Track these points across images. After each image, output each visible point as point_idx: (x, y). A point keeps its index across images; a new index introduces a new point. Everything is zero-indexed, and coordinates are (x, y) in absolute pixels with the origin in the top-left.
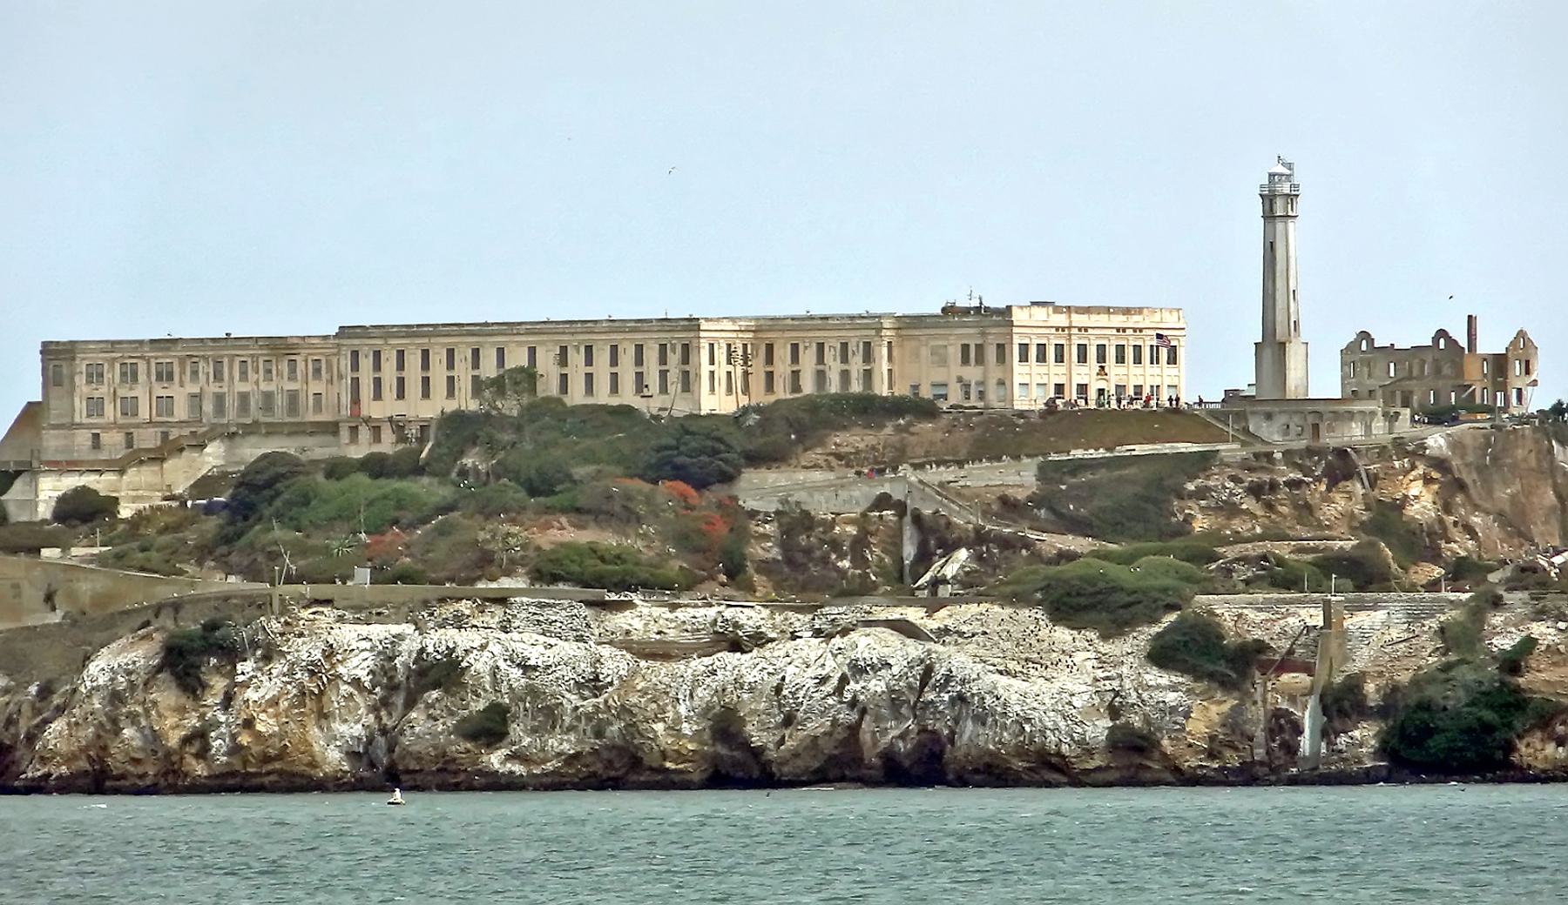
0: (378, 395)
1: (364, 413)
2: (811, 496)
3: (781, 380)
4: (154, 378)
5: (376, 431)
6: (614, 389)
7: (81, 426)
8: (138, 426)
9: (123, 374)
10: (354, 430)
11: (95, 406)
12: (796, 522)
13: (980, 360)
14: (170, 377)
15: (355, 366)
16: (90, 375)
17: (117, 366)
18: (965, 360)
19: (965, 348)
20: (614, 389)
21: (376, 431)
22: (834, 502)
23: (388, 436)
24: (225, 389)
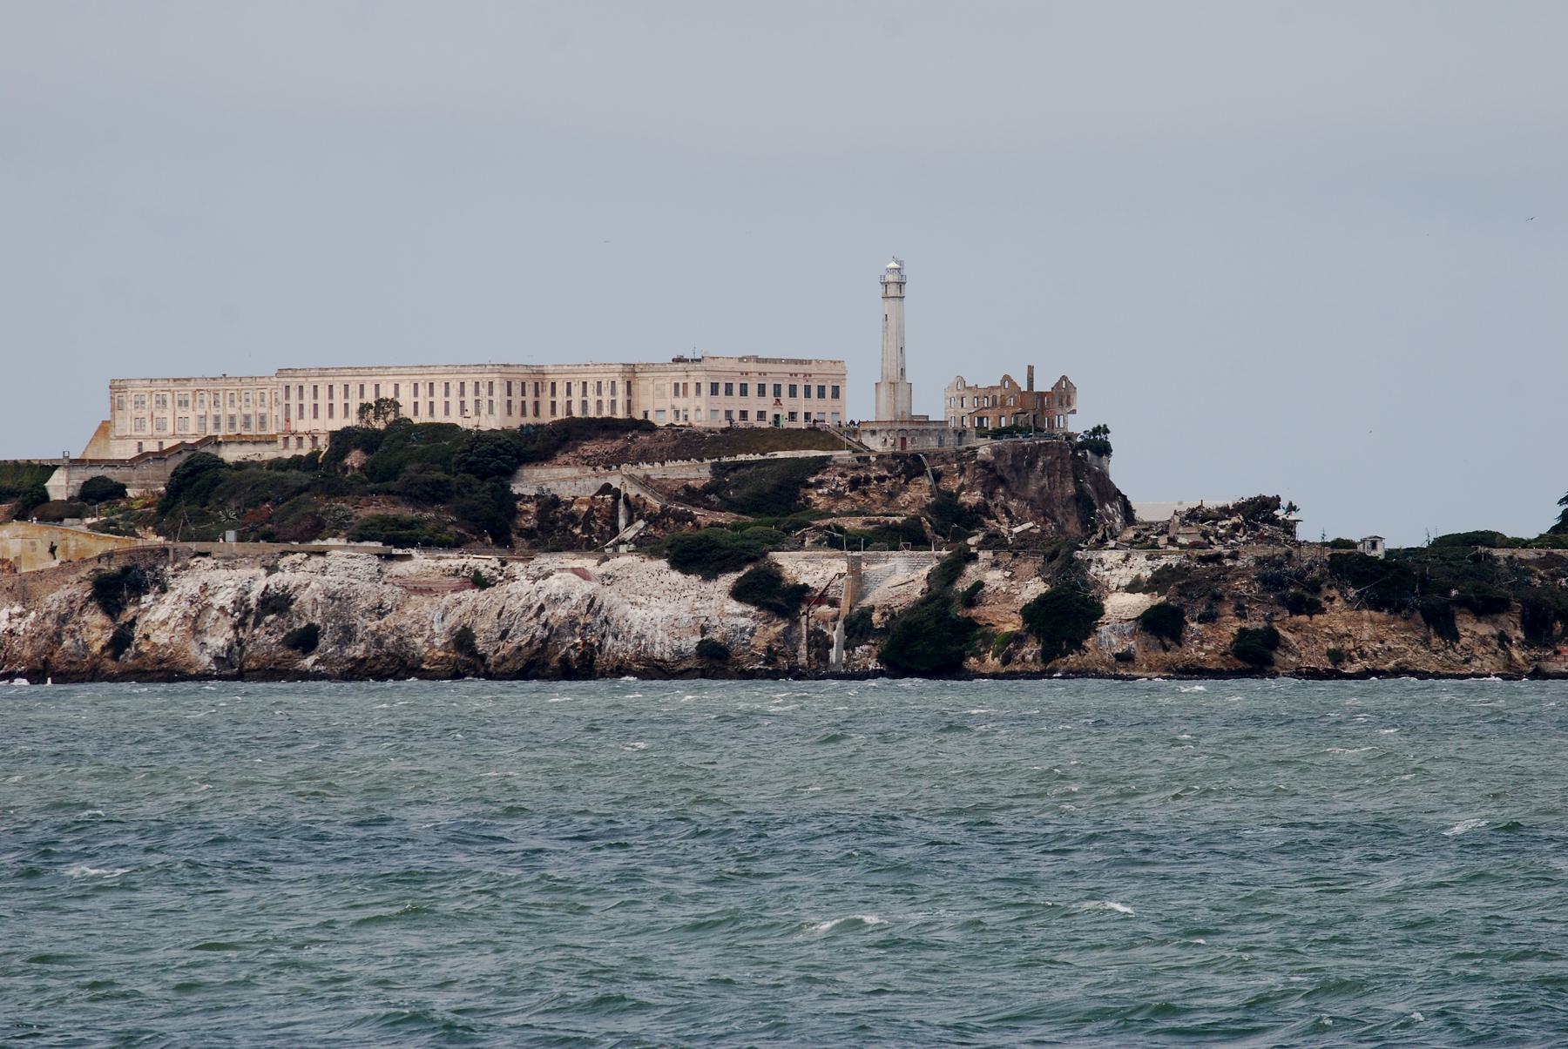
0: (301, 416)
4: (176, 405)
5: (300, 439)
6: (447, 412)
7: (130, 437)
9: (158, 402)
10: (286, 439)
11: (140, 422)
12: (549, 504)
13: (685, 394)
14: (186, 403)
15: (287, 397)
17: (154, 396)
18: (677, 394)
19: (677, 385)
20: (447, 412)
21: (300, 439)
23: (307, 443)
24: (221, 413)
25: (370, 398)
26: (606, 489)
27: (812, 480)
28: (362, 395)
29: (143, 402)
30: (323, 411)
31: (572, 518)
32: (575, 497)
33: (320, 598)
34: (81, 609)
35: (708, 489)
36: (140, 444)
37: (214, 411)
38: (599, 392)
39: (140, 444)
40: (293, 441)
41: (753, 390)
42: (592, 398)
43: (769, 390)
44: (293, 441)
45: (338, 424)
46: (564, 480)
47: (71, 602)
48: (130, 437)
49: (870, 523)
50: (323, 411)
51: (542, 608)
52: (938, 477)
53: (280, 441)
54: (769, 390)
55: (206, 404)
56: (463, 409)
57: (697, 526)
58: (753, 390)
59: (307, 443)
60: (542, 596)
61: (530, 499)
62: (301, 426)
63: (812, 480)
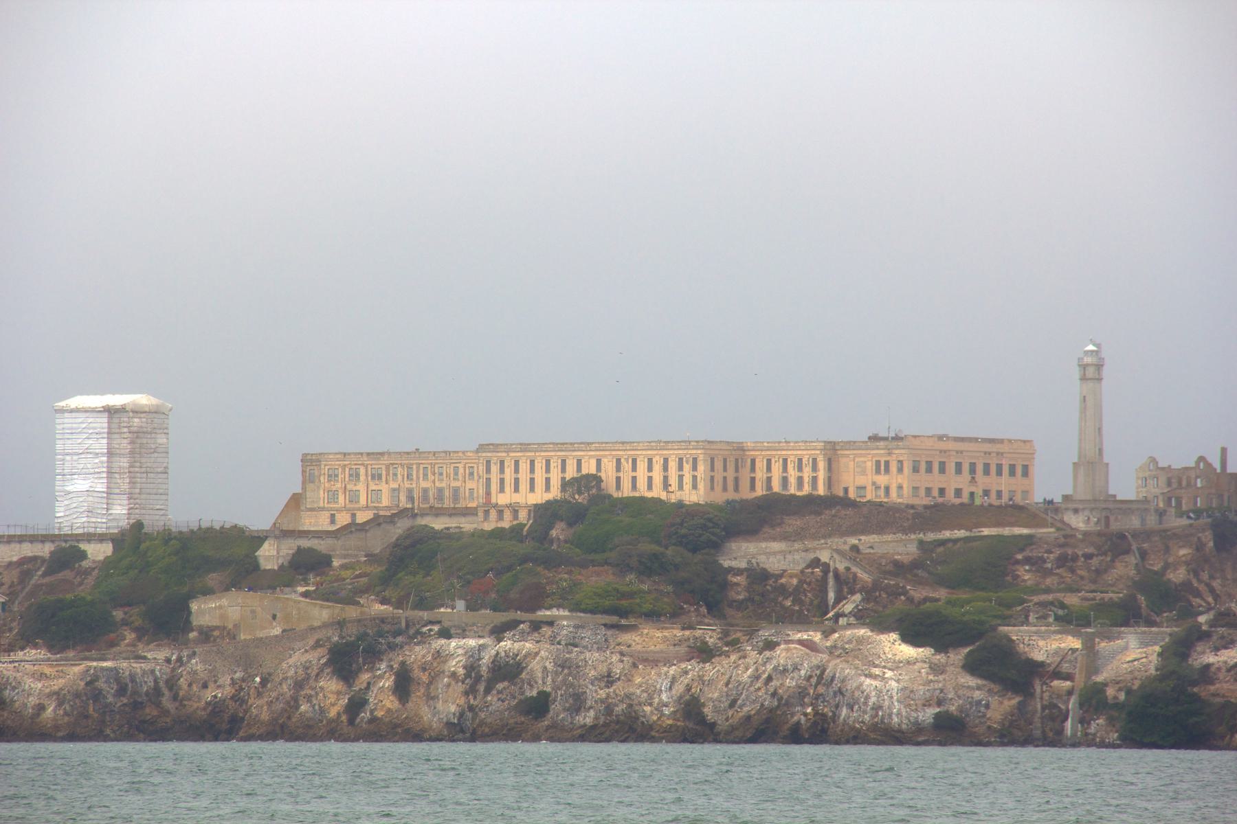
0: (502, 490)
1: (493, 501)
2: (768, 559)
3: (760, 483)
4: (370, 478)
5: (500, 513)
6: (650, 487)
7: (323, 509)
8: (359, 509)
9: (350, 475)
10: (487, 513)
11: (333, 495)
12: (759, 576)
13: (887, 470)
14: (380, 477)
15: (488, 470)
16: (330, 476)
17: (347, 470)
18: (878, 471)
19: (878, 463)
20: (650, 487)
21: (500, 513)
22: (783, 562)
23: (508, 515)
24: (414, 486)
25: (571, 473)
26: (816, 562)
27: (1019, 557)
28: (564, 470)
29: (337, 476)
30: (524, 486)
31: (782, 590)
32: (785, 571)
33: (550, 666)
34: (317, 675)
35: (916, 565)
36: (333, 516)
37: (407, 485)
38: (800, 469)
39: (333, 516)
40: (493, 514)
41: (951, 467)
42: (792, 474)
43: (966, 468)
44: (493, 514)
45: (539, 497)
46: (775, 553)
47: (307, 668)
48: (323, 509)
49: (1086, 599)
50: (524, 486)
51: (770, 679)
52: (1143, 555)
53: (481, 514)
54: (966, 468)
55: (400, 477)
56: (666, 485)
57: (910, 600)
58: (951, 467)
59: (508, 515)
60: (770, 667)
61: (739, 572)
62: (503, 499)
63: (1019, 557)
